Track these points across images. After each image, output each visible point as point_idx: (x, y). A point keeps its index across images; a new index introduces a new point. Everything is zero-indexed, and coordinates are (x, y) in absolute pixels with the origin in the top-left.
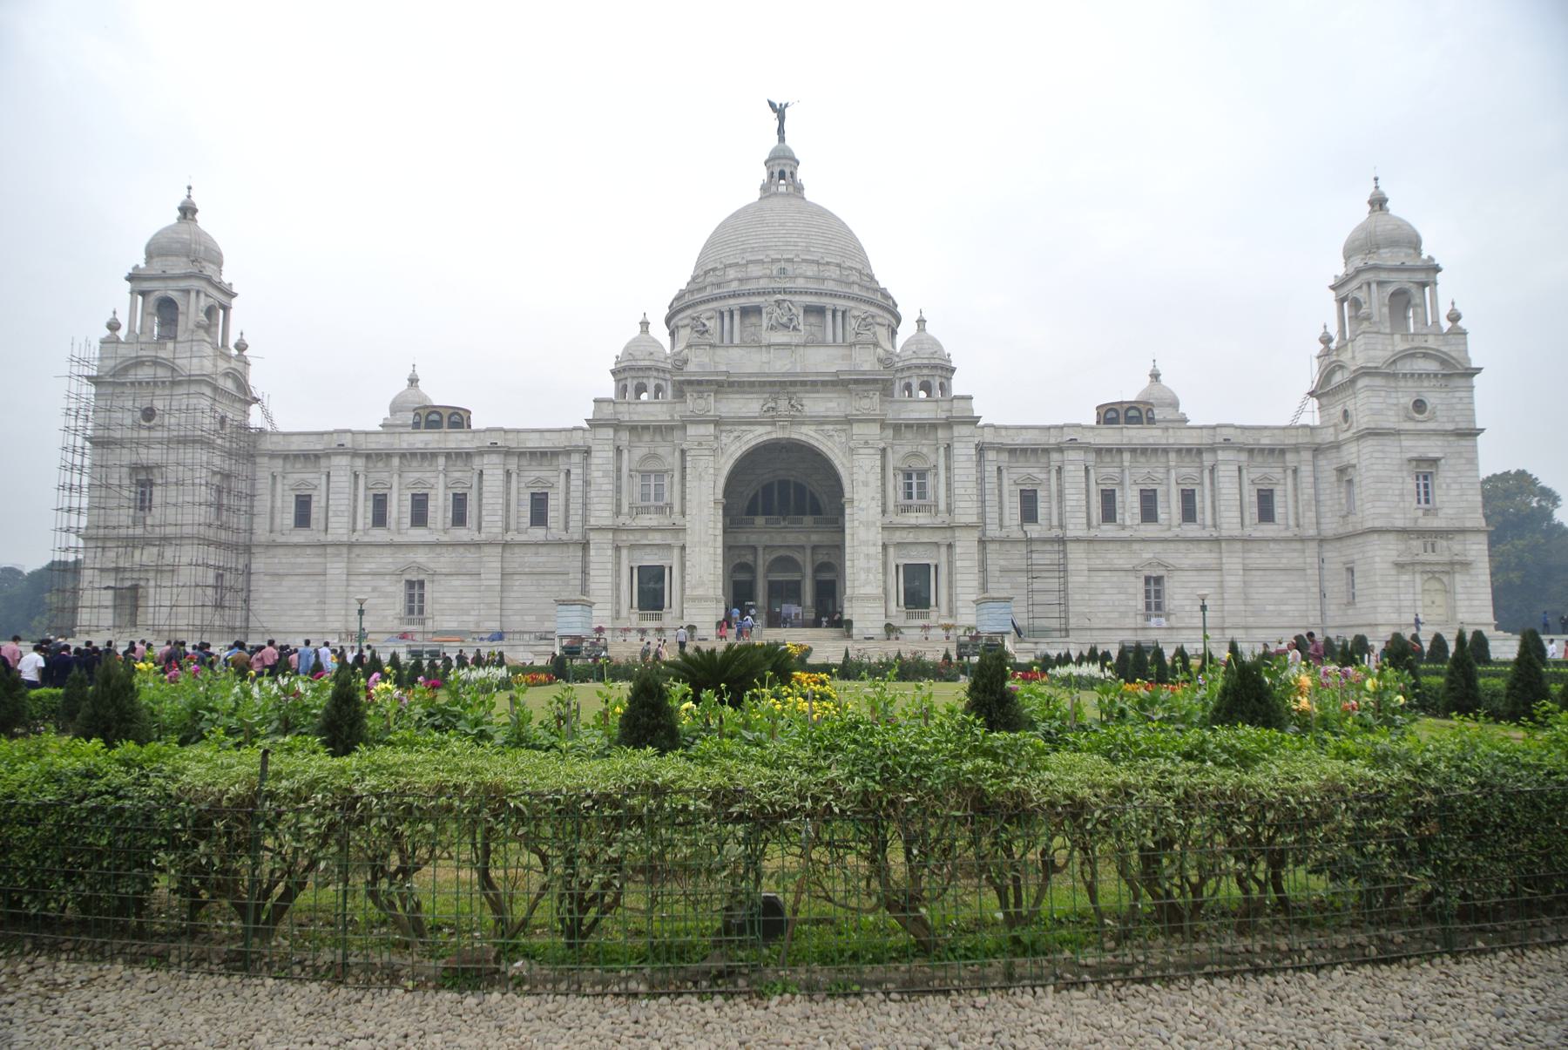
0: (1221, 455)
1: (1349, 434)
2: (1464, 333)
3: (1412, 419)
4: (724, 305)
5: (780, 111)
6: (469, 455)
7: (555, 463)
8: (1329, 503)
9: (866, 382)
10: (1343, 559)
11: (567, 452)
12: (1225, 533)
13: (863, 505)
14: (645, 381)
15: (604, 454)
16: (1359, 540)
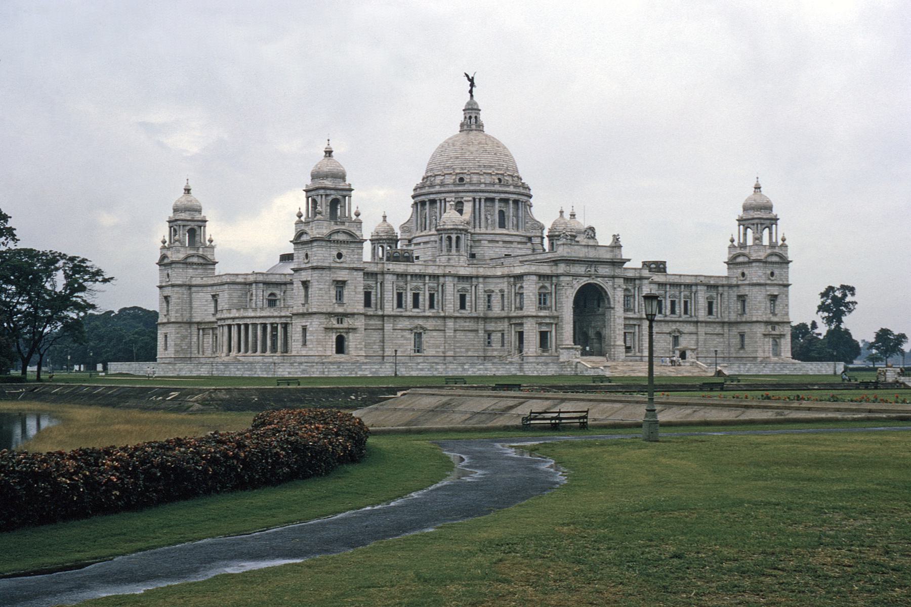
0: (699, 288)
1: (747, 282)
2: (787, 246)
3: (770, 279)
4: (478, 196)
5: (472, 81)
6: (438, 276)
7: (470, 281)
8: (733, 308)
9: (621, 262)
10: (738, 331)
11: (477, 277)
12: (701, 319)
13: (617, 310)
14: (459, 235)
15: (532, 286)
16: (749, 324)
